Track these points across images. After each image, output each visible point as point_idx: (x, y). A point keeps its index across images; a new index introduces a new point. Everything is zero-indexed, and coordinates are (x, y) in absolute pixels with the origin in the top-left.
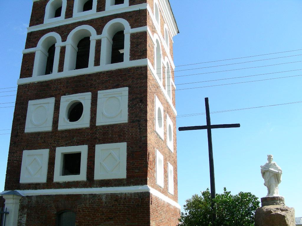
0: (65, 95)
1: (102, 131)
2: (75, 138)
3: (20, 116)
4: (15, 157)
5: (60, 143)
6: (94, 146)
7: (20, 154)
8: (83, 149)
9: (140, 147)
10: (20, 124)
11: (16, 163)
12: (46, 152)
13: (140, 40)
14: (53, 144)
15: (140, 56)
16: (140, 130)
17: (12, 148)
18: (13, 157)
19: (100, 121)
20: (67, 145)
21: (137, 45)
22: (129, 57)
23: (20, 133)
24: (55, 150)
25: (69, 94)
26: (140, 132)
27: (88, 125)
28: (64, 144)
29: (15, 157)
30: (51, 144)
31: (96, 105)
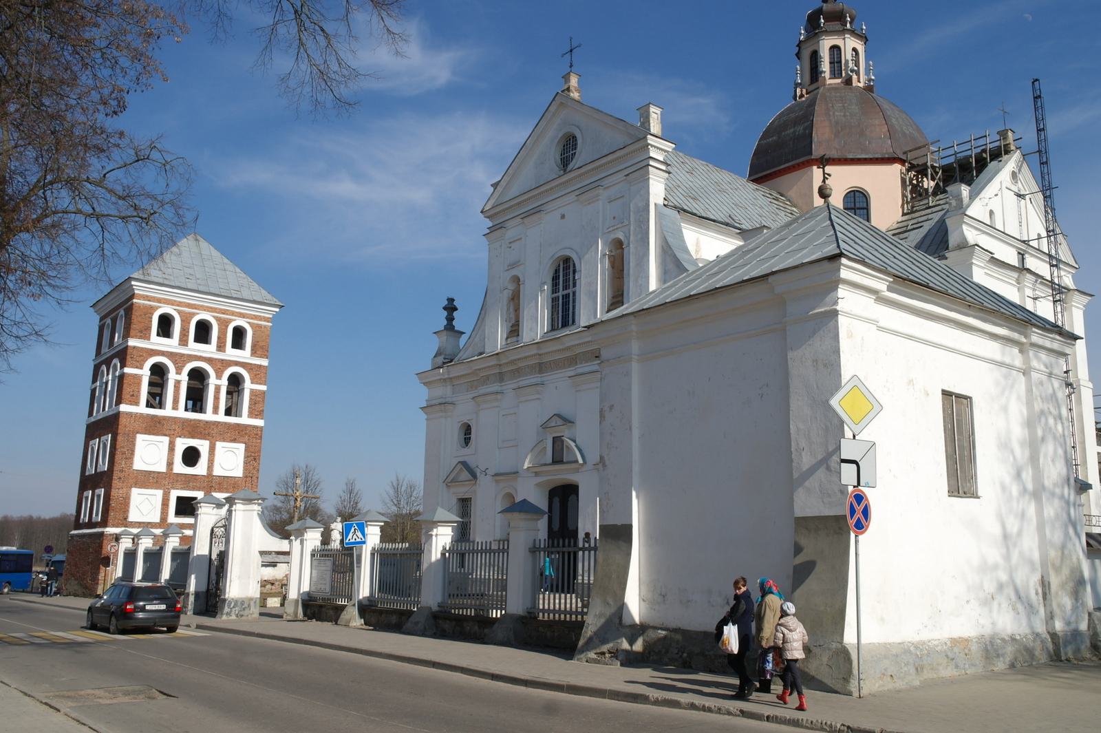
0: (180, 437)
10: (126, 458)
12: (159, 493)
13: (258, 399)
15: (257, 415)
19: (218, 471)
20: (182, 489)
21: (256, 403)
22: (247, 413)
25: (185, 437)
27: (205, 473)
31: (214, 455)
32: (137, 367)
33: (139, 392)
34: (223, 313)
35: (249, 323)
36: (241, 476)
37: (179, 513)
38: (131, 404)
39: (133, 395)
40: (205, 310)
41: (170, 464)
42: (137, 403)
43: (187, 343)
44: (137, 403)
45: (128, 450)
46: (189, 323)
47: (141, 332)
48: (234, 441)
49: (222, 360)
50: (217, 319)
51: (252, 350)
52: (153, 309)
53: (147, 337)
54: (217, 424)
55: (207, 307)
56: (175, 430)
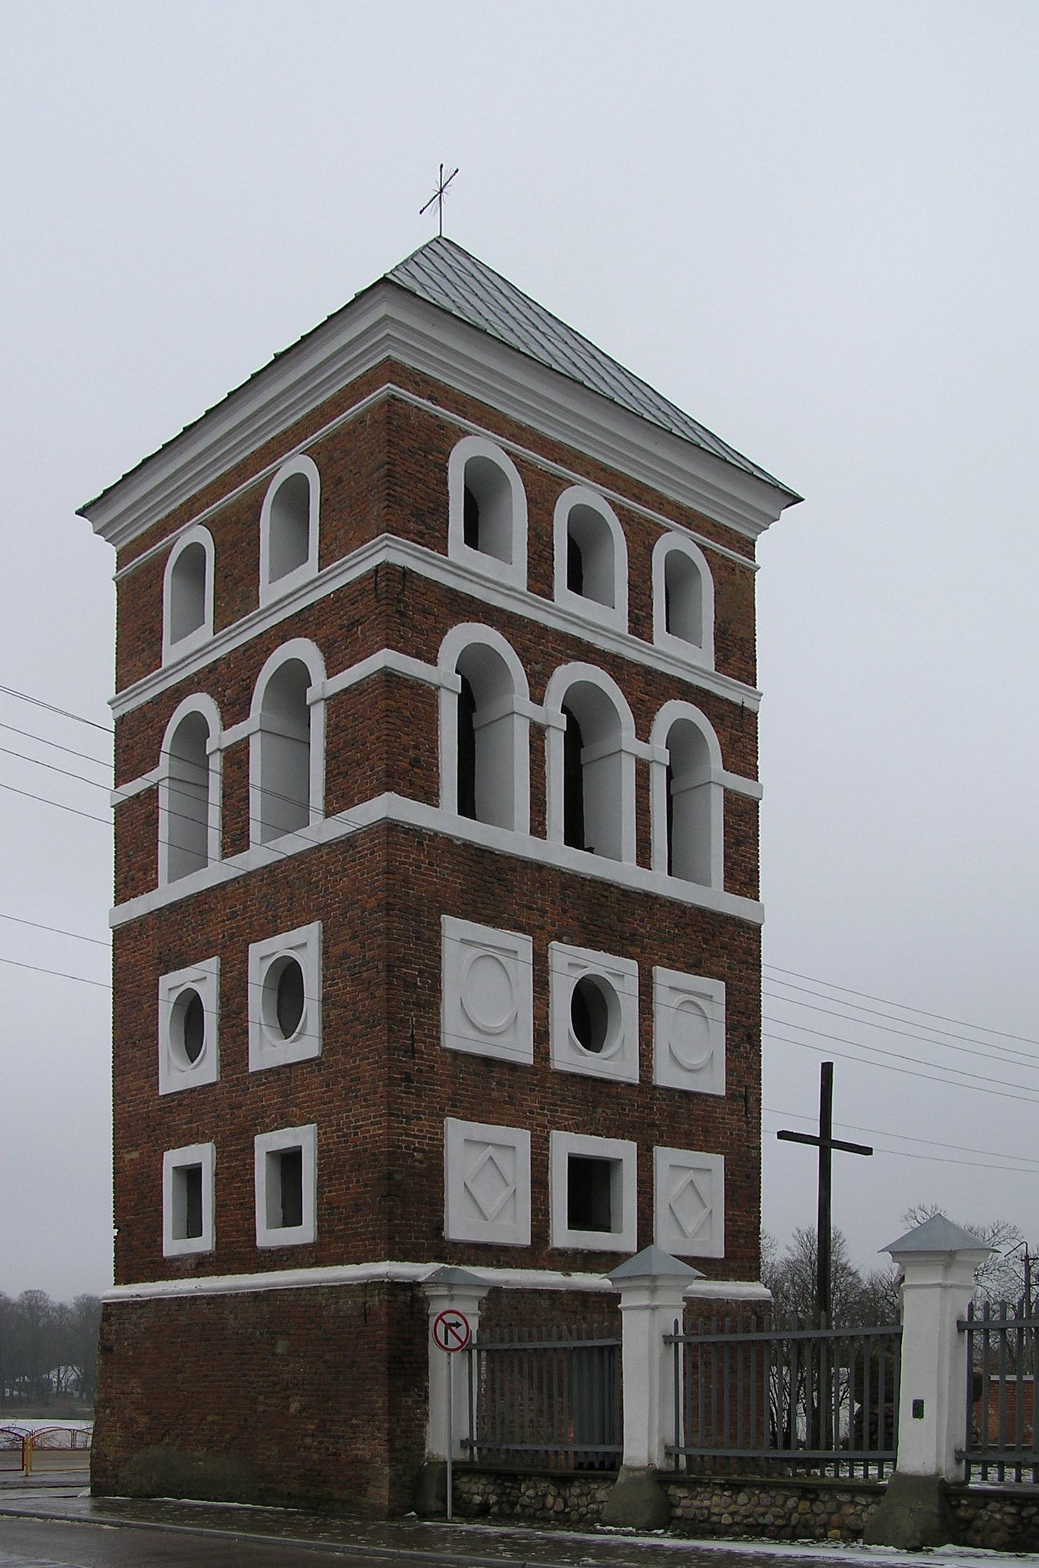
1: (666, 1105)
2: (600, 1110)
3: (415, 969)
4: (415, 1136)
5: (560, 1118)
6: (650, 1150)
7: (430, 1126)
8: (623, 1150)
9: (748, 1176)
10: (419, 1005)
11: (421, 1162)
14: (538, 1114)
16: (747, 1127)
17: (401, 1098)
18: (407, 1135)
19: (665, 1076)
23: (425, 1042)
24: (547, 1140)
26: (748, 1132)
28: (571, 1122)
29: (415, 1136)
30: (531, 1112)
32: (418, 656)
33: (433, 750)
34: (637, 498)
35: (703, 549)
36: (722, 1092)
37: (578, 1219)
38: (414, 797)
39: (415, 763)
40: (587, 474)
41: (542, 1036)
42: (430, 796)
43: (551, 587)
44: (430, 796)
45: (421, 972)
46: (551, 515)
47: (419, 516)
48: (695, 968)
49: (649, 671)
50: (625, 516)
51: (717, 650)
52: (447, 436)
53: (439, 543)
54: (648, 899)
55: (594, 462)
56: (543, 912)
